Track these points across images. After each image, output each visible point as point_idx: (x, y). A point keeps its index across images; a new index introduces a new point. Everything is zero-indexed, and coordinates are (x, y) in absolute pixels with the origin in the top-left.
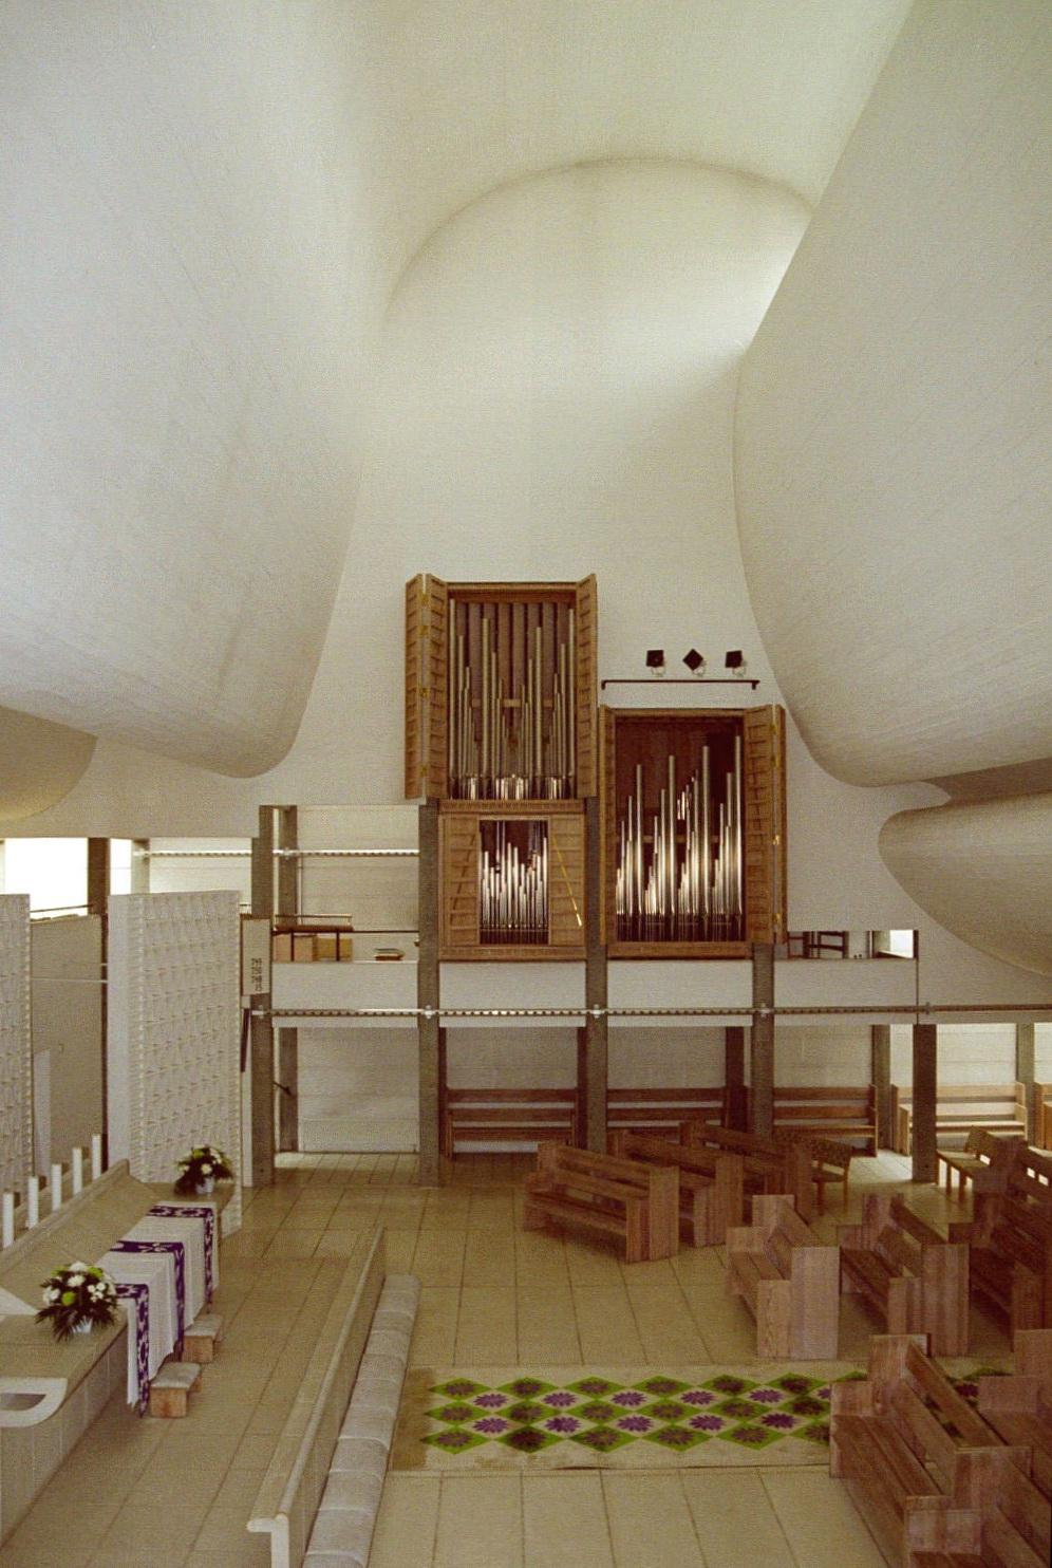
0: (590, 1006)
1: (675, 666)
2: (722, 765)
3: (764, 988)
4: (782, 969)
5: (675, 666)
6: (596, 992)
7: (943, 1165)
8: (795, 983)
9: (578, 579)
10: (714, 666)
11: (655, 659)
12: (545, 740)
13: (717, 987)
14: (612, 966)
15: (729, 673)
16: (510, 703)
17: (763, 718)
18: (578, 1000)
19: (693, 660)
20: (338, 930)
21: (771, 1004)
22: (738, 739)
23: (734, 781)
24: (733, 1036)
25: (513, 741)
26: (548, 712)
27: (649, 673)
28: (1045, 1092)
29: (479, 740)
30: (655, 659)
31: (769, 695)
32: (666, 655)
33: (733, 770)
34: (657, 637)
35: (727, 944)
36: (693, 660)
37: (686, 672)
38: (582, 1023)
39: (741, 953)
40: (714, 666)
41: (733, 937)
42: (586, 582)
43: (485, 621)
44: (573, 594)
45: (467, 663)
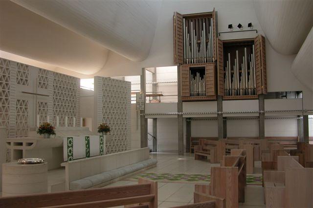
0: (218, 111)
3: (262, 107)
4: (268, 102)
6: (220, 108)
8: (271, 105)
9: (212, 11)
15: (249, 28)
16: (199, 42)
17: (258, 39)
19: (240, 26)
21: (264, 110)
23: (253, 56)
25: (199, 51)
27: (229, 30)
29: (191, 50)
30: (230, 26)
31: (261, 33)
36: (240, 26)
37: (238, 29)
39: (256, 97)
45: (196, 35)
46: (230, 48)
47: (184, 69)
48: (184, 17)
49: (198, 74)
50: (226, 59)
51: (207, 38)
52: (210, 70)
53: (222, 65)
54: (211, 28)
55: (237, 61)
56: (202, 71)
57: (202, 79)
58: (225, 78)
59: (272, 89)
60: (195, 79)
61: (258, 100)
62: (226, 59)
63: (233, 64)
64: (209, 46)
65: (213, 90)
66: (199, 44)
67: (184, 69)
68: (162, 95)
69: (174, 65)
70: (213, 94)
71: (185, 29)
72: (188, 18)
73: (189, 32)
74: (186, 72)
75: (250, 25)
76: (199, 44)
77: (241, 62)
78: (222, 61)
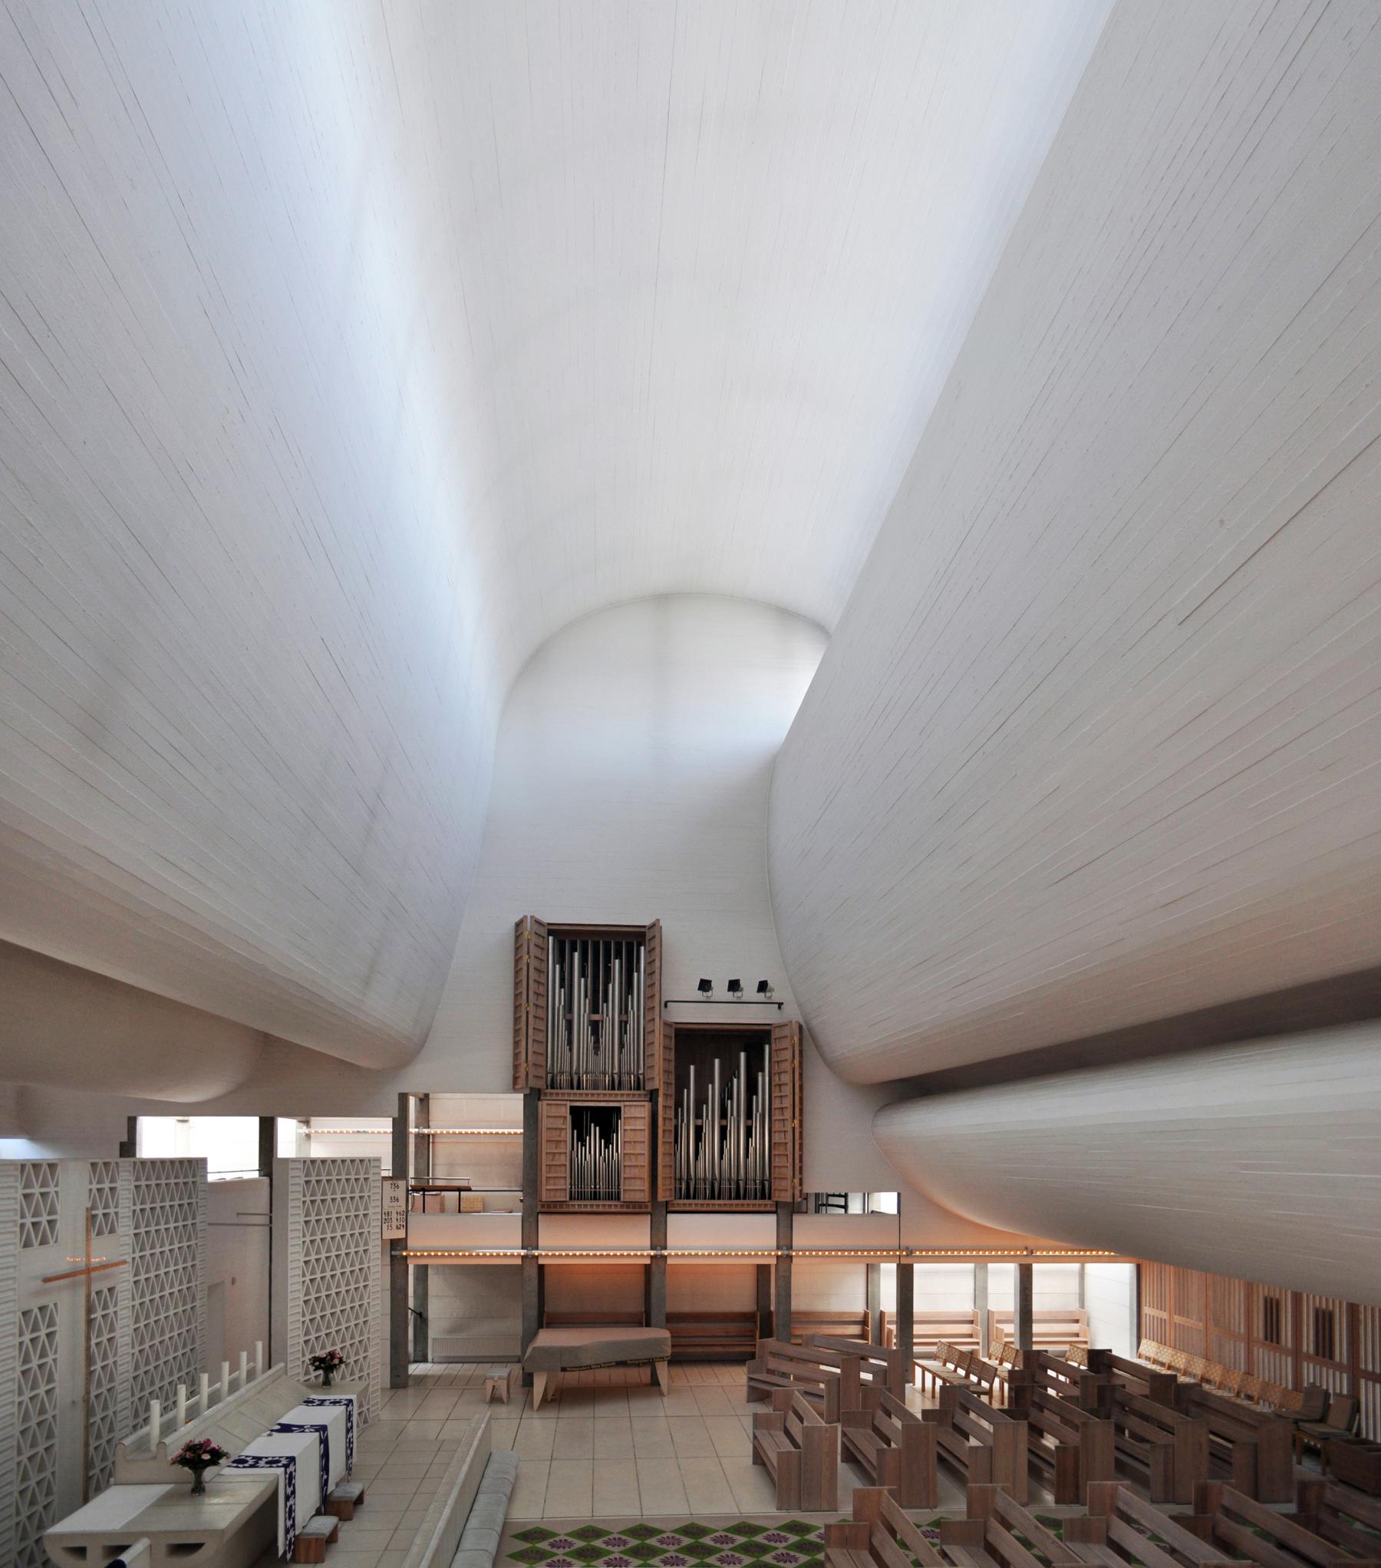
1: (720, 990)
2: (755, 1066)
3: (785, 1238)
5: (720, 990)
6: (659, 1239)
7: (918, 1371)
9: (647, 923)
10: (749, 991)
11: (705, 985)
12: (622, 1046)
13: (746, 1236)
14: (671, 1218)
15: (761, 997)
16: (596, 1017)
17: (786, 1031)
18: (646, 1241)
20: (459, 1189)
21: (790, 1247)
22: (767, 1047)
23: (763, 1080)
24: (762, 1271)
25: (596, 1048)
26: (623, 1024)
28: (996, 1317)
29: (570, 1043)
30: (705, 985)
31: (792, 1013)
32: (713, 984)
33: (763, 1071)
34: (705, 967)
35: (758, 1202)
38: (648, 1261)
39: (768, 1209)
40: (749, 991)
41: (763, 1197)
42: (653, 925)
43: (576, 955)
44: (644, 934)
46: (695, 1045)
47: (554, 1111)
48: (550, 932)
49: (595, 1131)
50: (681, 1083)
51: (624, 1010)
52: (635, 1118)
53: (672, 1102)
54: (640, 978)
55: (714, 1090)
56: (607, 1120)
57: (606, 1147)
58: (676, 1142)
59: (813, 1186)
60: (584, 1145)
61: (773, 1218)
62: (681, 1083)
63: (701, 1101)
64: (629, 1037)
65: (645, 1185)
66: (595, 1027)
67: (554, 1111)
68: (469, 1189)
69: (515, 1087)
70: (645, 1197)
71: (553, 970)
72: (570, 941)
73: (566, 982)
74: (559, 1124)
75: (763, 986)
76: (595, 1027)
77: (726, 1093)
78: (672, 1090)
